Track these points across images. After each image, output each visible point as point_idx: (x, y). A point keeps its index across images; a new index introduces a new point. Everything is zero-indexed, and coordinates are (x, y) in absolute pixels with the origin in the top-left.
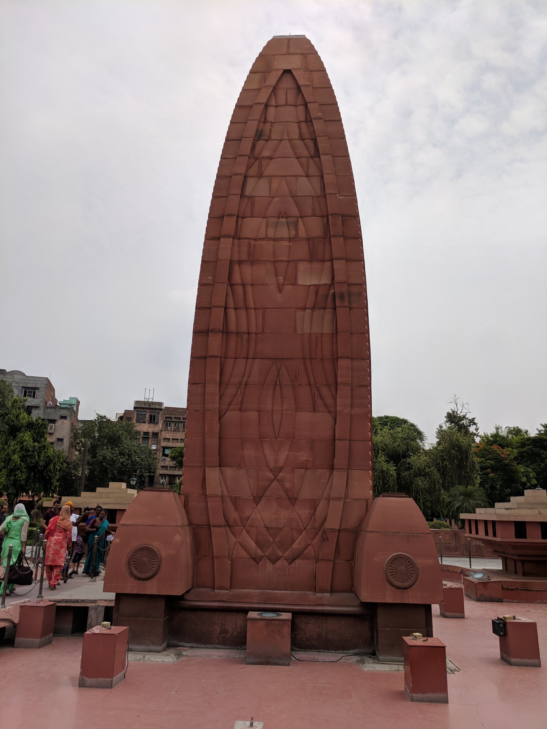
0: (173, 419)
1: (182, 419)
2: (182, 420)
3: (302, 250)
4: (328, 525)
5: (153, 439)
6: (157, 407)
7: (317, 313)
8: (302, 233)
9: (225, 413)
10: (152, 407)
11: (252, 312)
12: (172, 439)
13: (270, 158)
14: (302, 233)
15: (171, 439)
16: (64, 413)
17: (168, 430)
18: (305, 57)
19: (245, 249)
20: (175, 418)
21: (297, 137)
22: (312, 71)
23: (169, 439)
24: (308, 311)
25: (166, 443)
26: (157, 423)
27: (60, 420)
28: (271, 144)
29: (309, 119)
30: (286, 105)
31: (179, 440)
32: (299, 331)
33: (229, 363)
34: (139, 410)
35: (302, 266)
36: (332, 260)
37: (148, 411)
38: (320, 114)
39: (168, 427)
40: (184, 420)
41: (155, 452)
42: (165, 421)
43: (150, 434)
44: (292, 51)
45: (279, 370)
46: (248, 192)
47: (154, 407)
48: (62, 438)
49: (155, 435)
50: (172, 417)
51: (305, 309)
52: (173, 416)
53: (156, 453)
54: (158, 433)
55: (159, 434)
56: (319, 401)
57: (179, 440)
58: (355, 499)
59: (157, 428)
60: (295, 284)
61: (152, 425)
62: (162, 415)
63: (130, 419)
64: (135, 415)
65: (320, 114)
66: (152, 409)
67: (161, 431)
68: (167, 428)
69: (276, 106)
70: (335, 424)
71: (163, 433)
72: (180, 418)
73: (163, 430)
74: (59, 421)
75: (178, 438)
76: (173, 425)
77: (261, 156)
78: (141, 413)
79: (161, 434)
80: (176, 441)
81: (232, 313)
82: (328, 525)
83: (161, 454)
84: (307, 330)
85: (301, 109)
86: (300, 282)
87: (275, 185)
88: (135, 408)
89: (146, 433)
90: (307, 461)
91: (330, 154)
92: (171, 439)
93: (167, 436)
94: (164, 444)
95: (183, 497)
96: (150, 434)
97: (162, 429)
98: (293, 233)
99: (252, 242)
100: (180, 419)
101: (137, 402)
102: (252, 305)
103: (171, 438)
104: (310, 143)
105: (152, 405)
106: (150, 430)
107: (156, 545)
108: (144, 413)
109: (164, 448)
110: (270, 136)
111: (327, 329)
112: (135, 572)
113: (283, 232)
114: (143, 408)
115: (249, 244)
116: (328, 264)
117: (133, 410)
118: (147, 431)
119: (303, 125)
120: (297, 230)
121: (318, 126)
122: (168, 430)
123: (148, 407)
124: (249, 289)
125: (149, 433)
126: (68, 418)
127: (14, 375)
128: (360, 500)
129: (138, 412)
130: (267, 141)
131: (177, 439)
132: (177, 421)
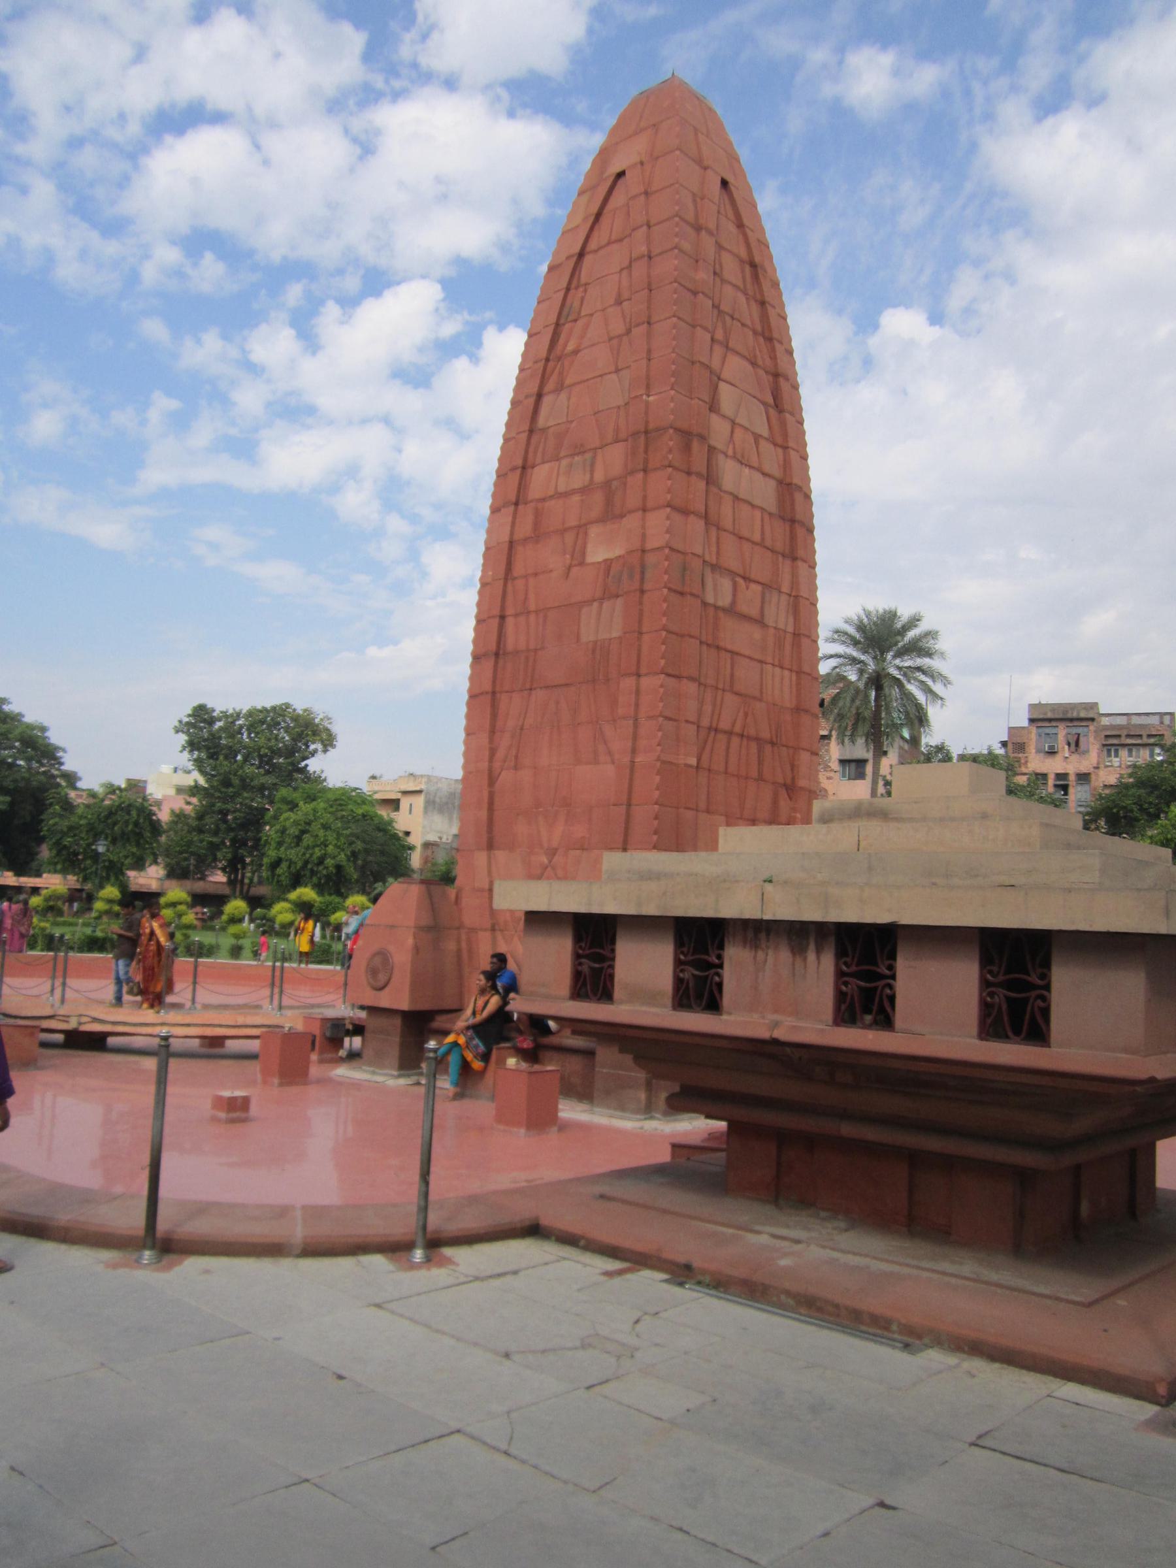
2: (1145, 740)
5: (1079, 788)
6: (1083, 715)
8: (599, 477)
9: (500, 773)
10: (1069, 716)
13: (576, 352)
17: (1112, 766)
26: (1087, 751)
33: (504, 699)
34: (1040, 724)
35: (594, 531)
37: (1062, 726)
40: (1152, 741)
42: (1104, 745)
43: (1072, 778)
47: (1075, 715)
49: (1083, 778)
52: (1124, 733)
54: (1089, 774)
55: (1093, 777)
60: (582, 563)
61: (1075, 757)
63: (1021, 747)
64: (1033, 736)
66: (1071, 720)
67: (1097, 768)
68: (1111, 761)
72: (1140, 736)
73: (1102, 766)
76: (1124, 753)
77: (566, 352)
78: (1047, 731)
79: (1097, 775)
84: (592, 638)
88: (1032, 721)
90: (583, 837)
91: (643, 323)
96: (1072, 778)
97: (1098, 763)
101: (1033, 707)
102: (532, 607)
105: (1070, 712)
108: (1053, 731)
114: (1050, 720)
117: (1025, 723)
118: (1063, 772)
123: (1061, 716)
129: (1041, 730)
130: (575, 321)
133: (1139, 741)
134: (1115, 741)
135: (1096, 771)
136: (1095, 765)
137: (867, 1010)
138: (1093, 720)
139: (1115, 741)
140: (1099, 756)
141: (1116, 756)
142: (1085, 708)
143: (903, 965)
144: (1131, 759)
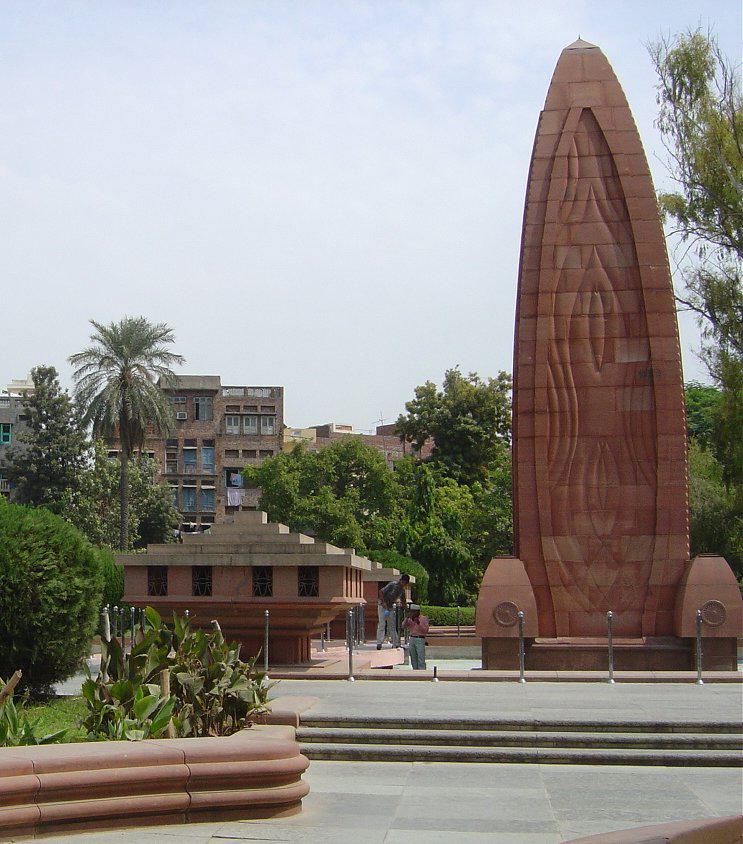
2: (260, 412)
4: (652, 582)
7: (638, 390)
15: (240, 452)
24: (628, 389)
25: (232, 460)
29: (615, 173)
31: (258, 453)
32: (620, 409)
36: (648, 337)
45: (603, 448)
46: (560, 264)
51: (625, 386)
52: (242, 404)
57: (258, 453)
70: (656, 495)
75: (253, 448)
82: (652, 582)
86: (617, 361)
92: (240, 452)
111: (646, 407)
116: (644, 341)
119: (610, 181)
121: (625, 182)
131: (255, 451)
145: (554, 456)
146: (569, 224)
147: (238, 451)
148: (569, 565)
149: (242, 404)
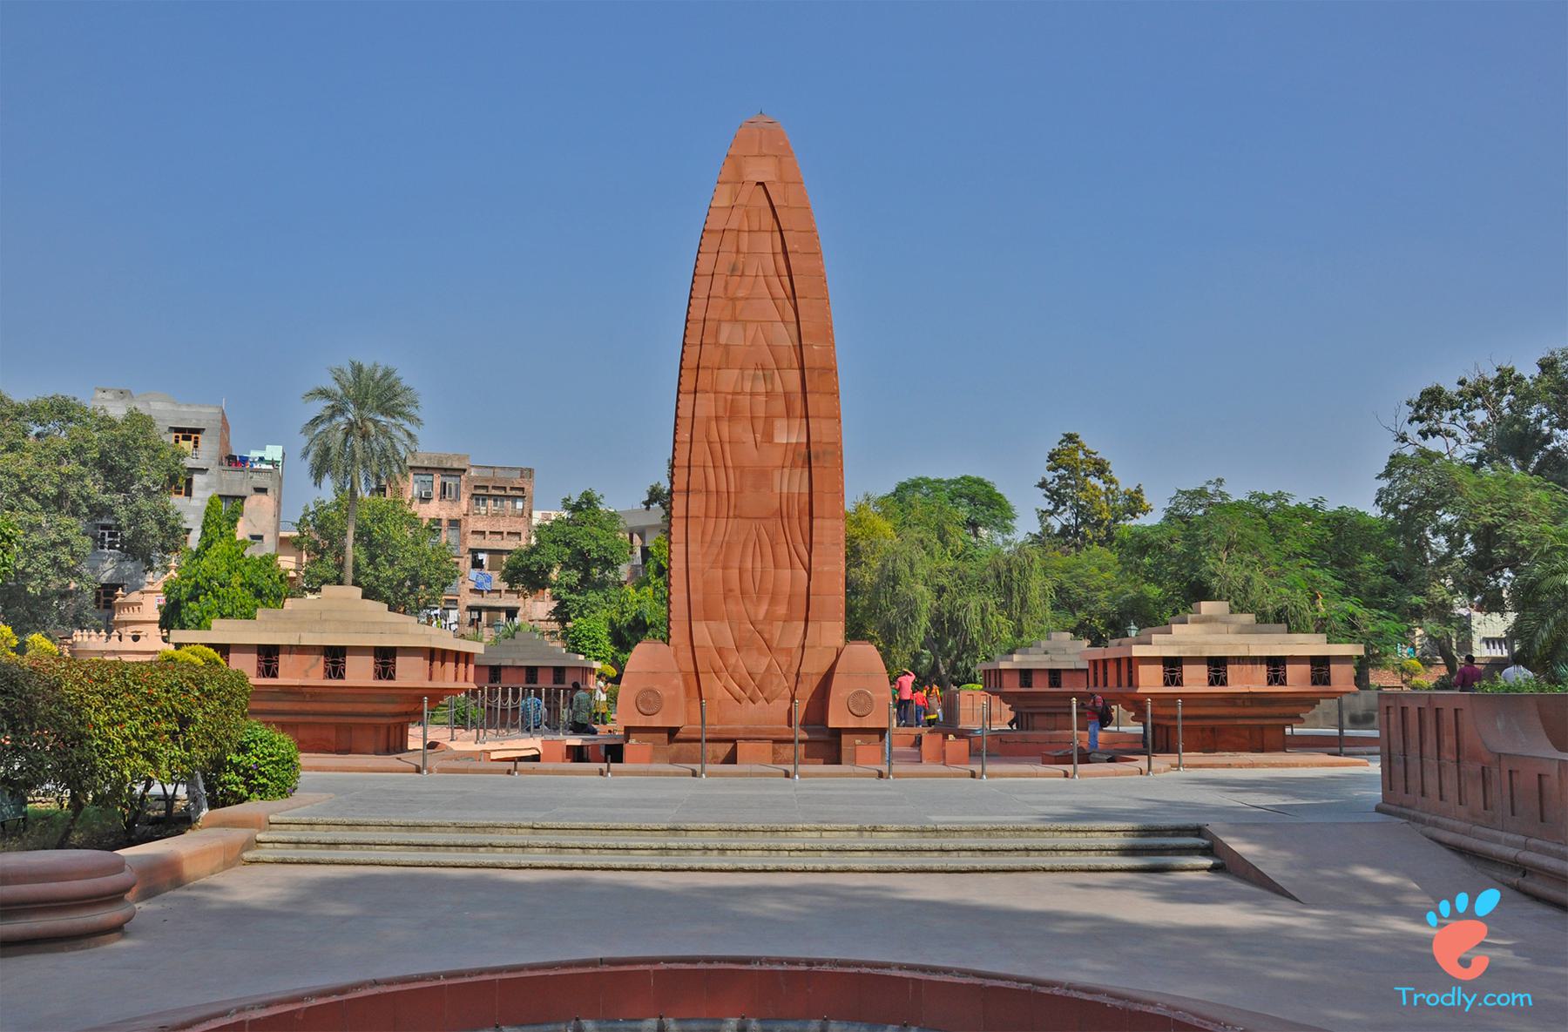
0: (490, 488)
1: (508, 489)
2: (510, 493)
3: (779, 406)
5: (450, 532)
11: (731, 472)
12: (491, 532)
14: (779, 388)
15: (487, 533)
16: (259, 480)
17: (480, 514)
18: (780, 161)
19: (721, 404)
20: (494, 488)
21: (772, 273)
22: (787, 183)
23: (484, 532)
27: (254, 496)
28: (747, 280)
30: (760, 230)
34: (417, 471)
38: (796, 246)
39: (482, 508)
40: (514, 493)
41: (456, 560)
42: (473, 495)
43: (444, 523)
44: (765, 151)
46: (723, 340)
47: (448, 466)
48: (260, 533)
49: (455, 523)
50: (487, 487)
52: (491, 485)
53: (457, 563)
55: (463, 523)
56: (796, 559)
58: (826, 647)
59: (456, 510)
61: (445, 504)
62: (466, 482)
65: (796, 246)
66: (446, 470)
67: (467, 515)
68: (479, 509)
69: (749, 231)
71: (470, 520)
72: (505, 489)
73: (470, 513)
74: (252, 498)
75: (502, 530)
76: (490, 502)
78: (423, 478)
80: (499, 537)
81: (711, 471)
83: (469, 563)
85: (777, 235)
87: (750, 333)
89: (438, 521)
93: (480, 527)
94: (474, 542)
95: (672, 648)
96: (444, 523)
97: (468, 511)
98: (769, 387)
99: (730, 397)
100: (505, 491)
103: (487, 529)
104: (786, 280)
106: (444, 515)
107: (657, 687)
108: (430, 478)
109: (474, 552)
110: (743, 272)
112: (642, 709)
113: (761, 387)
114: (426, 468)
115: (726, 400)
120: (773, 384)
122: (480, 514)
124: (727, 447)
125: (440, 520)
126: (270, 492)
127: (151, 403)
128: (830, 647)
129: (417, 477)
131: (502, 533)
132: (498, 496)
133: (503, 493)
134: (483, 492)
135: (465, 517)
136: (465, 513)
137: (1276, 682)
138: (465, 470)
139: (483, 492)
140: (468, 504)
141: (484, 505)
142: (459, 459)
143: (1332, 666)
144: (496, 508)
145: (708, 538)
146: (734, 299)
147: (484, 532)
148: (720, 651)
149: (491, 485)
